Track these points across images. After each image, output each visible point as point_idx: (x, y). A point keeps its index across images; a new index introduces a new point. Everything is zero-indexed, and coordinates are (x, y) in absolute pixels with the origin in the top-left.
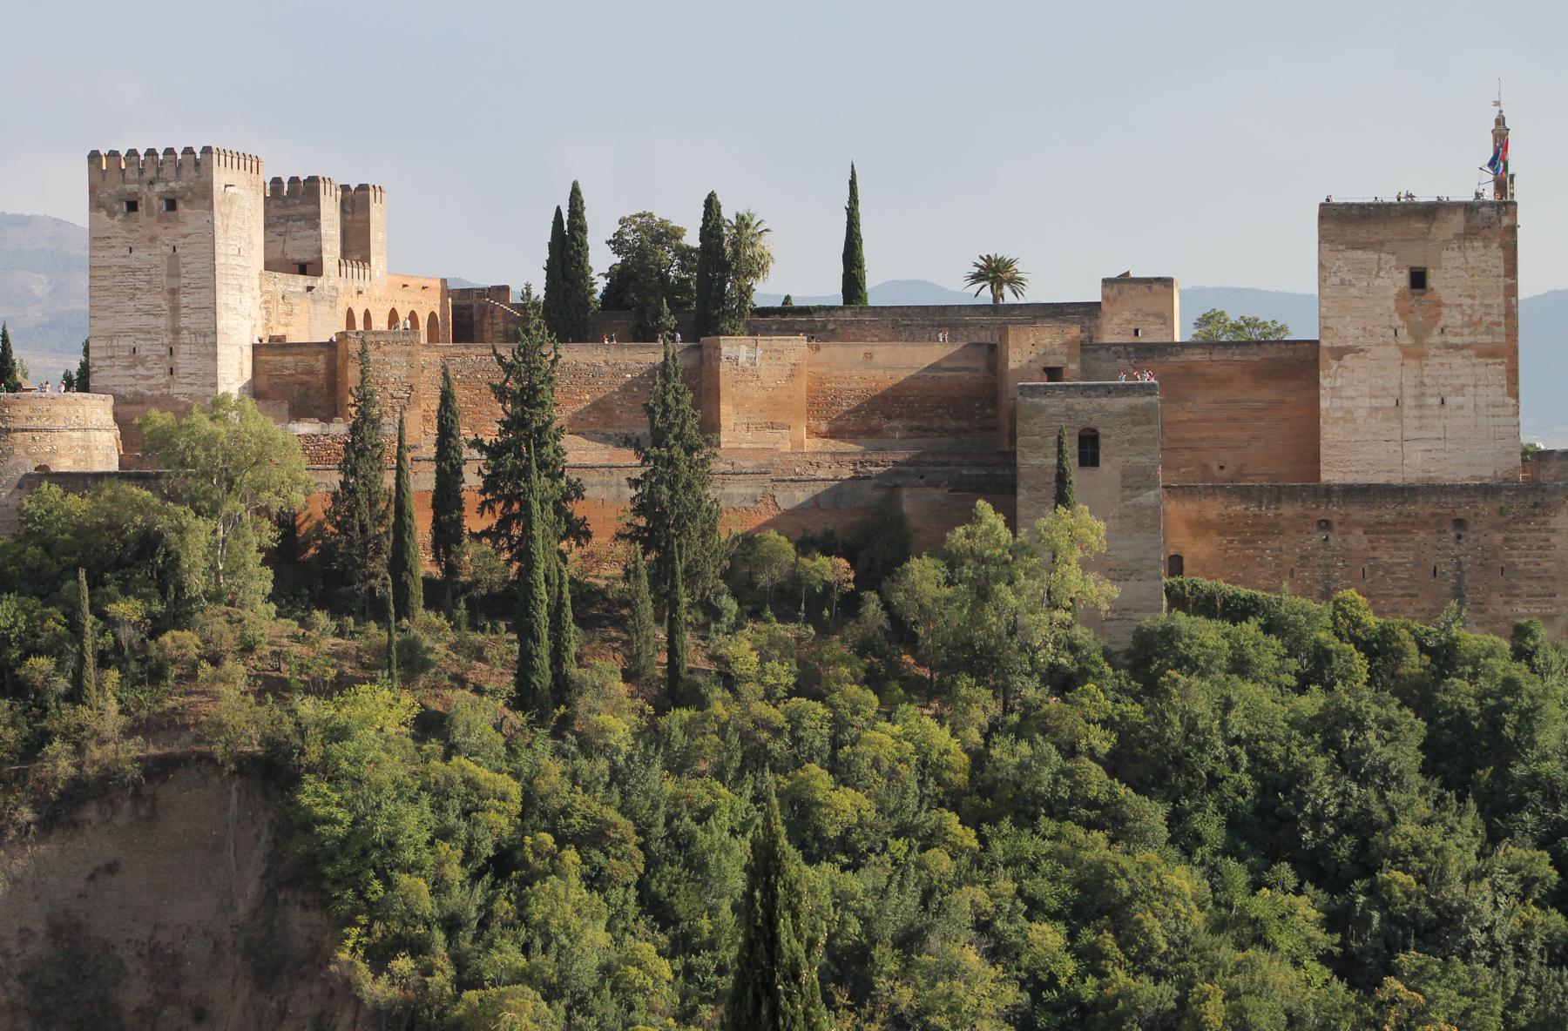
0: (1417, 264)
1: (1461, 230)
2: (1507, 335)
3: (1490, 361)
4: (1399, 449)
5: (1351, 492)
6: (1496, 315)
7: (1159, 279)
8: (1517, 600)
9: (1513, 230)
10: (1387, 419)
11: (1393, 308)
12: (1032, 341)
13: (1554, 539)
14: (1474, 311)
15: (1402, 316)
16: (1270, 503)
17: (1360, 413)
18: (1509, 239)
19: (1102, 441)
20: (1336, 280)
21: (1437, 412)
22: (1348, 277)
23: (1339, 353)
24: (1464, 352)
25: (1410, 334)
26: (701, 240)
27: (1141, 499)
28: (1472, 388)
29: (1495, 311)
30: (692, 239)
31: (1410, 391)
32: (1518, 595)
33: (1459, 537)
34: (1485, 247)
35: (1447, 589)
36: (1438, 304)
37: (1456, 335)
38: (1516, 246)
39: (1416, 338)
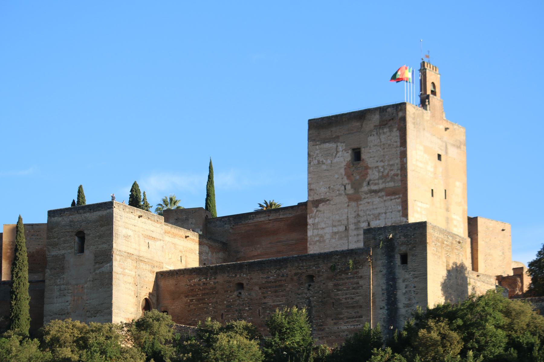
0: (355, 146)
1: (377, 123)
2: (402, 181)
3: (393, 197)
6: (396, 170)
8: (341, 322)
10: (341, 238)
11: (344, 173)
13: (361, 282)
14: (384, 169)
15: (349, 176)
17: (328, 236)
18: (402, 125)
20: (315, 162)
25: (352, 187)
27: (103, 269)
28: (384, 215)
29: (396, 167)
31: (352, 220)
32: (342, 319)
33: (310, 285)
36: (367, 168)
37: (375, 184)
39: (355, 189)
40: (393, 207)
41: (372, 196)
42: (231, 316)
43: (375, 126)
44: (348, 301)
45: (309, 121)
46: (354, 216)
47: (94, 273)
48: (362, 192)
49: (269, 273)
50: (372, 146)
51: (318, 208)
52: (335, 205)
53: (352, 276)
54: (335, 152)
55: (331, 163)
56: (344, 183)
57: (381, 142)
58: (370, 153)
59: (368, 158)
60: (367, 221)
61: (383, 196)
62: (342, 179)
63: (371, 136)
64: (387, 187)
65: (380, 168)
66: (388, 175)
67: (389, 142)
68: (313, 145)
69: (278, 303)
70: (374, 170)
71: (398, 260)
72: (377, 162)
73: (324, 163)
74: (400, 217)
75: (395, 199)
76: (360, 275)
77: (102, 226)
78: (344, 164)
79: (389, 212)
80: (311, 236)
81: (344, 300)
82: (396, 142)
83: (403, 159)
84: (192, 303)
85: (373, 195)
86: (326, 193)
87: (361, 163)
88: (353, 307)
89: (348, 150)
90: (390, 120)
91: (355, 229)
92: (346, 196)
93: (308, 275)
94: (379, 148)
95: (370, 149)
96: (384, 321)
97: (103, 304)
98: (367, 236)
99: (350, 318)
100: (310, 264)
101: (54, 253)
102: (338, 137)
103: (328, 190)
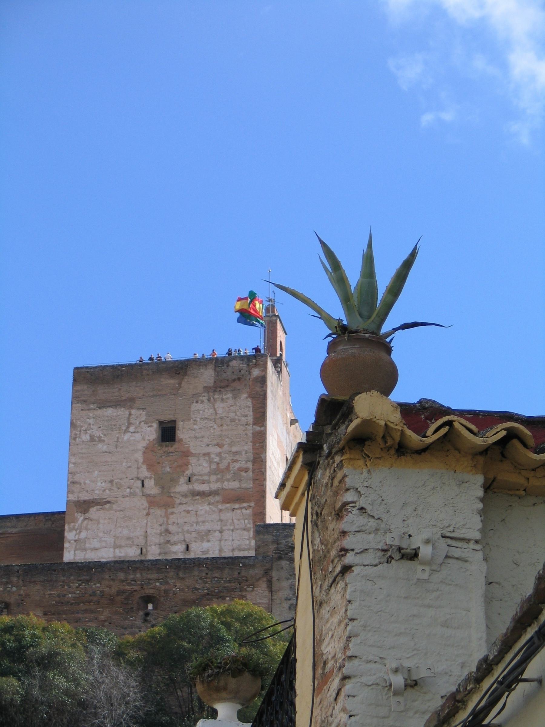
2: (254, 480)
3: (237, 506)
11: (141, 460)
14: (221, 459)
15: (150, 467)
18: (258, 389)
20: (86, 437)
22: (98, 433)
25: (156, 484)
28: (217, 533)
29: (244, 456)
34: (235, 397)
36: (187, 454)
39: (163, 488)
40: (235, 521)
41: (196, 501)
43: (205, 387)
45: (76, 369)
46: (158, 532)
48: (175, 492)
49: (66, 587)
50: (198, 419)
55: (118, 442)
56: (141, 476)
57: (216, 413)
62: (138, 468)
64: (225, 487)
66: (228, 467)
67: (232, 415)
68: (82, 410)
70: (202, 459)
72: (208, 445)
73: (104, 441)
75: (241, 508)
78: (142, 445)
79: (229, 530)
82: (246, 416)
86: (104, 490)
87: (176, 445)
90: (234, 380)
92: (144, 498)
93: (144, 597)
95: (194, 424)
98: (262, 536)
100: (149, 576)
102: (132, 400)
103: (109, 485)
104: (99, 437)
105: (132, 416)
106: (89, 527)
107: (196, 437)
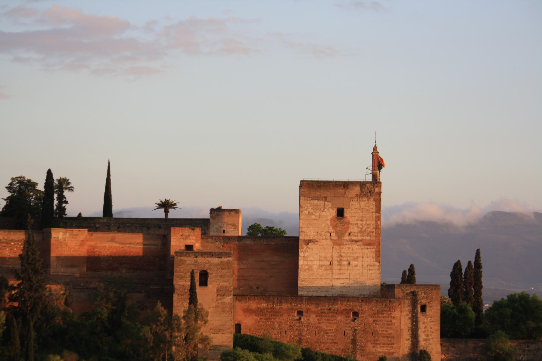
0: (340, 206)
3: (369, 247)
4: (331, 282)
5: (311, 299)
6: (371, 228)
7: (234, 210)
8: (378, 346)
9: (380, 193)
10: (326, 270)
12: (181, 234)
13: (394, 321)
14: (363, 226)
15: (333, 228)
16: (277, 303)
17: (315, 267)
18: (377, 197)
19: (210, 276)
20: (307, 212)
21: (346, 267)
22: (311, 211)
23: (308, 242)
24: (358, 243)
25: (336, 235)
26: (45, 187)
28: (361, 258)
29: (372, 226)
30: (41, 187)
31: (335, 259)
32: (378, 344)
34: (368, 200)
35: (349, 341)
36: (348, 223)
37: (355, 236)
38: (380, 200)
39: (339, 237)
42: (293, 333)
44: (383, 332)
45: (302, 181)
46: (337, 256)
47: (216, 302)
48: (344, 240)
50: (353, 209)
51: (308, 246)
52: (321, 245)
53: (387, 316)
54: (323, 208)
55: (320, 215)
57: (360, 207)
58: (352, 213)
59: (350, 216)
60: (347, 261)
61: (361, 245)
62: (328, 228)
63: (352, 201)
65: (359, 225)
67: (367, 208)
68: (305, 200)
69: (330, 328)
70: (355, 226)
71: (419, 310)
72: (357, 220)
73: (314, 215)
74: (374, 261)
75: (371, 248)
76: (393, 316)
77: (223, 269)
78: (330, 217)
79: (366, 257)
80: (301, 265)
81: (380, 331)
82: (373, 209)
83: (377, 222)
84: (261, 320)
85: (353, 243)
86: (315, 236)
87: (344, 219)
88: (387, 337)
89: (334, 208)
91: (338, 265)
92: (331, 241)
94: (358, 211)
96: (409, 349)
97: (224, 325)
99: (384, 344)
101: (181, 283)
103: (317, 234)
104: (312, 213)
105: (326, 205)
106: (309, 251)
107: (352, 216)
